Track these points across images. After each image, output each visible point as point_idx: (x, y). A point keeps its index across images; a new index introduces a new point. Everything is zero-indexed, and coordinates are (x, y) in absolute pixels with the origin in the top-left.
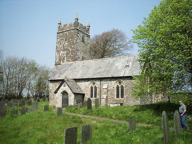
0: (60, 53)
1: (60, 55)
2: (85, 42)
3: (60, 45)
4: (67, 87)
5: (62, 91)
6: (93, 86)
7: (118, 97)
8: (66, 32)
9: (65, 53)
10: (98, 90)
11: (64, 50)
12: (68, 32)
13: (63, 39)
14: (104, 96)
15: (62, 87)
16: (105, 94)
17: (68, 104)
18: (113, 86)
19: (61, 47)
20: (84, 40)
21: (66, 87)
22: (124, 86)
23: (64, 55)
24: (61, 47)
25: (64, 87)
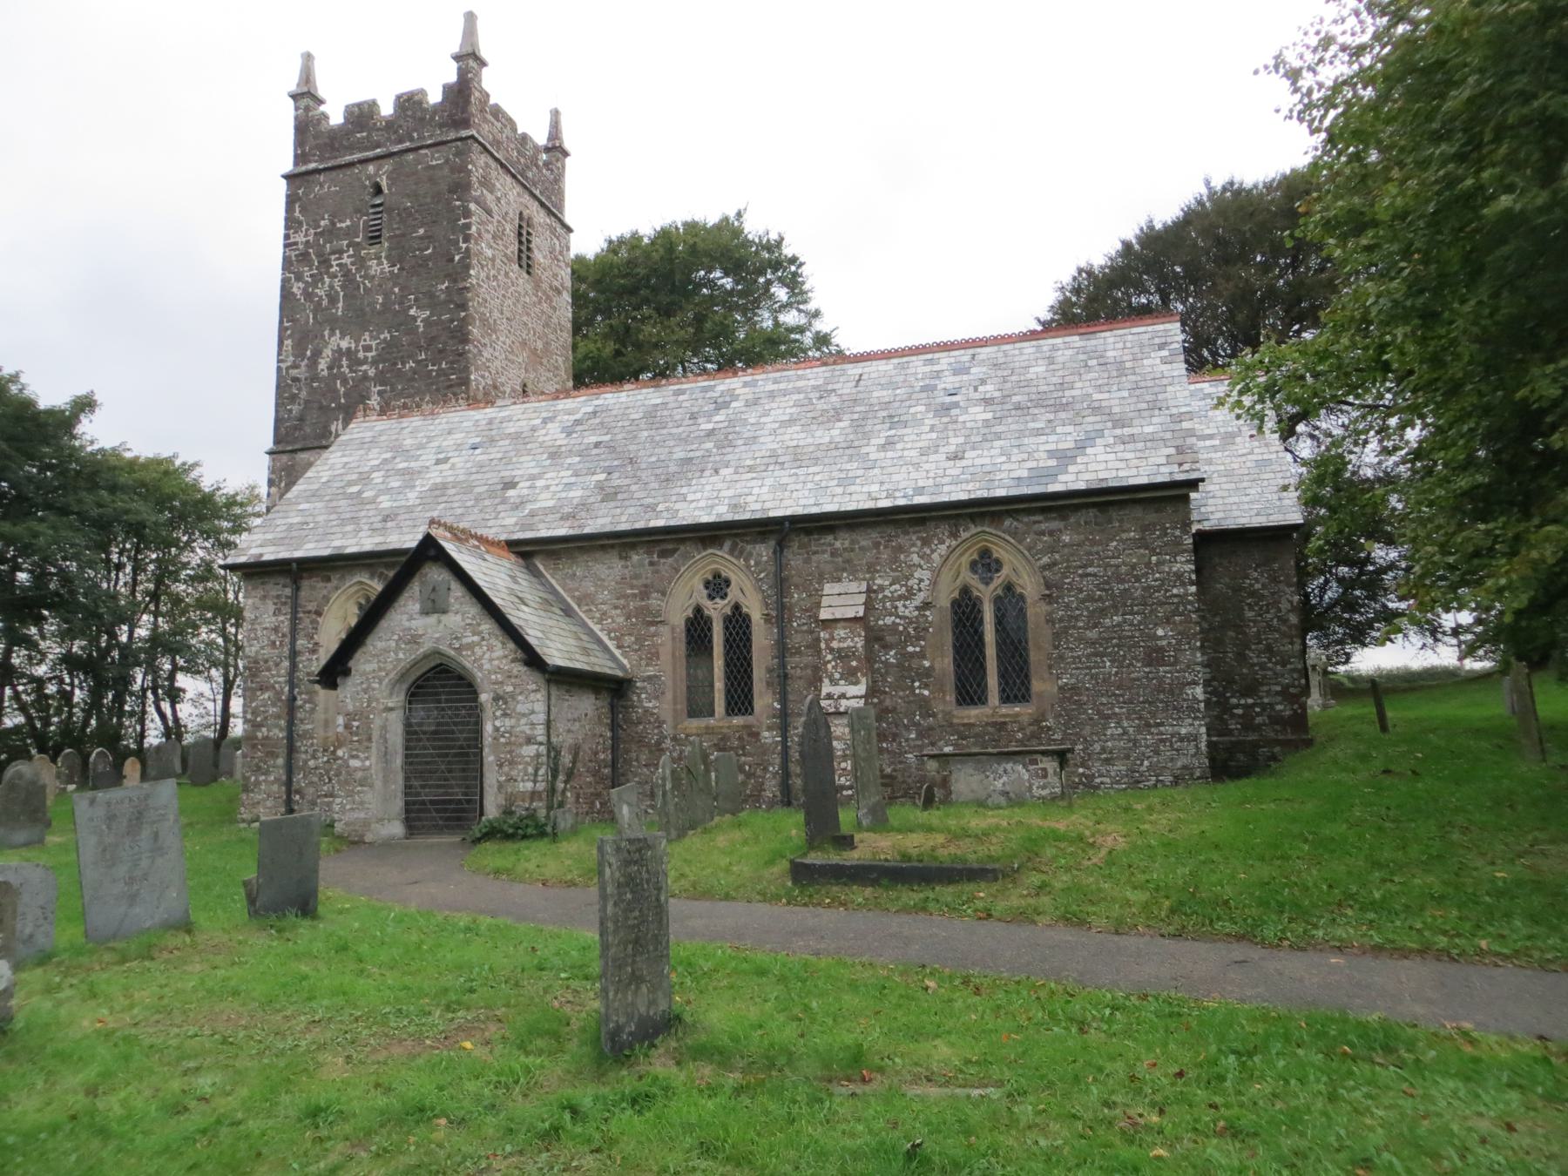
0: (317, 354)
1: (323, 365)
2: (537, 271)
3: (317, 280)
4: (461, 615)
5: (405, 657)
6: (717, 611)
7: (970, 692)
8: (371, 168)
9: (367, 349)
10: (762, 638)
11: (357, 320)
12: (387, 166)
13: (350, 233)
14: (836, 690)
15: (406, 616)
16: (850, 676)
17: (1295, 527)
18: (919, 599)
19: (333, 300)
20: (529, 249)
21: (453, 620)
22: (1030, 586)
23: (355, 362)
24: (333, 300)
25: (433, 619)
